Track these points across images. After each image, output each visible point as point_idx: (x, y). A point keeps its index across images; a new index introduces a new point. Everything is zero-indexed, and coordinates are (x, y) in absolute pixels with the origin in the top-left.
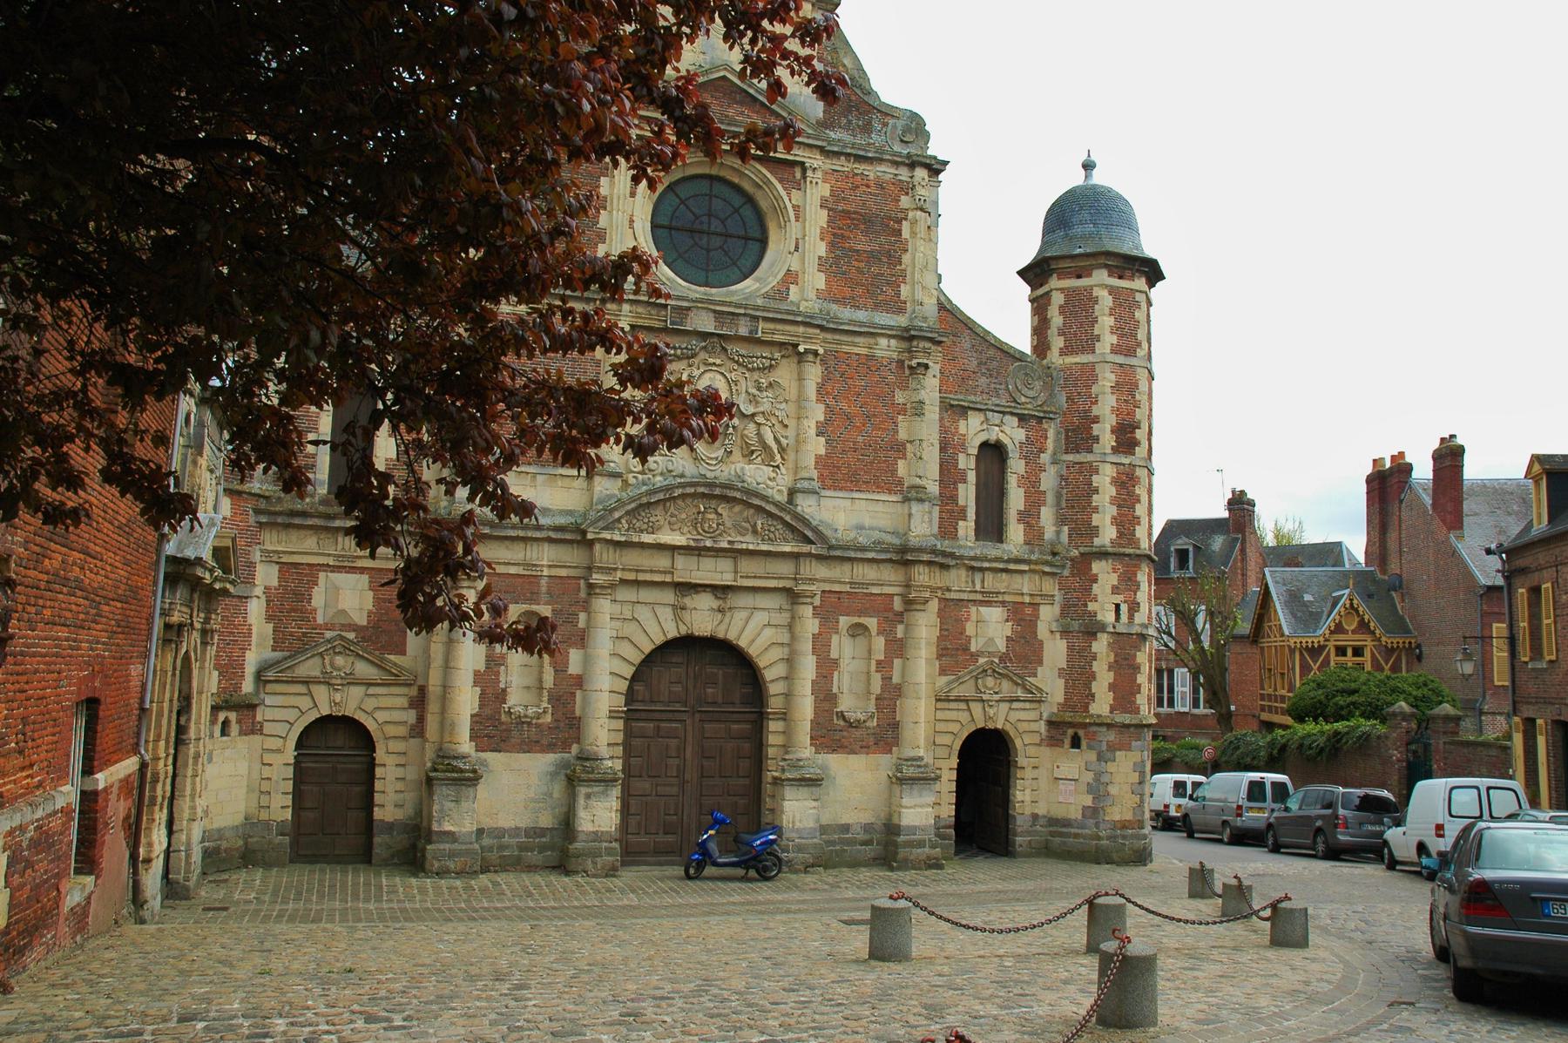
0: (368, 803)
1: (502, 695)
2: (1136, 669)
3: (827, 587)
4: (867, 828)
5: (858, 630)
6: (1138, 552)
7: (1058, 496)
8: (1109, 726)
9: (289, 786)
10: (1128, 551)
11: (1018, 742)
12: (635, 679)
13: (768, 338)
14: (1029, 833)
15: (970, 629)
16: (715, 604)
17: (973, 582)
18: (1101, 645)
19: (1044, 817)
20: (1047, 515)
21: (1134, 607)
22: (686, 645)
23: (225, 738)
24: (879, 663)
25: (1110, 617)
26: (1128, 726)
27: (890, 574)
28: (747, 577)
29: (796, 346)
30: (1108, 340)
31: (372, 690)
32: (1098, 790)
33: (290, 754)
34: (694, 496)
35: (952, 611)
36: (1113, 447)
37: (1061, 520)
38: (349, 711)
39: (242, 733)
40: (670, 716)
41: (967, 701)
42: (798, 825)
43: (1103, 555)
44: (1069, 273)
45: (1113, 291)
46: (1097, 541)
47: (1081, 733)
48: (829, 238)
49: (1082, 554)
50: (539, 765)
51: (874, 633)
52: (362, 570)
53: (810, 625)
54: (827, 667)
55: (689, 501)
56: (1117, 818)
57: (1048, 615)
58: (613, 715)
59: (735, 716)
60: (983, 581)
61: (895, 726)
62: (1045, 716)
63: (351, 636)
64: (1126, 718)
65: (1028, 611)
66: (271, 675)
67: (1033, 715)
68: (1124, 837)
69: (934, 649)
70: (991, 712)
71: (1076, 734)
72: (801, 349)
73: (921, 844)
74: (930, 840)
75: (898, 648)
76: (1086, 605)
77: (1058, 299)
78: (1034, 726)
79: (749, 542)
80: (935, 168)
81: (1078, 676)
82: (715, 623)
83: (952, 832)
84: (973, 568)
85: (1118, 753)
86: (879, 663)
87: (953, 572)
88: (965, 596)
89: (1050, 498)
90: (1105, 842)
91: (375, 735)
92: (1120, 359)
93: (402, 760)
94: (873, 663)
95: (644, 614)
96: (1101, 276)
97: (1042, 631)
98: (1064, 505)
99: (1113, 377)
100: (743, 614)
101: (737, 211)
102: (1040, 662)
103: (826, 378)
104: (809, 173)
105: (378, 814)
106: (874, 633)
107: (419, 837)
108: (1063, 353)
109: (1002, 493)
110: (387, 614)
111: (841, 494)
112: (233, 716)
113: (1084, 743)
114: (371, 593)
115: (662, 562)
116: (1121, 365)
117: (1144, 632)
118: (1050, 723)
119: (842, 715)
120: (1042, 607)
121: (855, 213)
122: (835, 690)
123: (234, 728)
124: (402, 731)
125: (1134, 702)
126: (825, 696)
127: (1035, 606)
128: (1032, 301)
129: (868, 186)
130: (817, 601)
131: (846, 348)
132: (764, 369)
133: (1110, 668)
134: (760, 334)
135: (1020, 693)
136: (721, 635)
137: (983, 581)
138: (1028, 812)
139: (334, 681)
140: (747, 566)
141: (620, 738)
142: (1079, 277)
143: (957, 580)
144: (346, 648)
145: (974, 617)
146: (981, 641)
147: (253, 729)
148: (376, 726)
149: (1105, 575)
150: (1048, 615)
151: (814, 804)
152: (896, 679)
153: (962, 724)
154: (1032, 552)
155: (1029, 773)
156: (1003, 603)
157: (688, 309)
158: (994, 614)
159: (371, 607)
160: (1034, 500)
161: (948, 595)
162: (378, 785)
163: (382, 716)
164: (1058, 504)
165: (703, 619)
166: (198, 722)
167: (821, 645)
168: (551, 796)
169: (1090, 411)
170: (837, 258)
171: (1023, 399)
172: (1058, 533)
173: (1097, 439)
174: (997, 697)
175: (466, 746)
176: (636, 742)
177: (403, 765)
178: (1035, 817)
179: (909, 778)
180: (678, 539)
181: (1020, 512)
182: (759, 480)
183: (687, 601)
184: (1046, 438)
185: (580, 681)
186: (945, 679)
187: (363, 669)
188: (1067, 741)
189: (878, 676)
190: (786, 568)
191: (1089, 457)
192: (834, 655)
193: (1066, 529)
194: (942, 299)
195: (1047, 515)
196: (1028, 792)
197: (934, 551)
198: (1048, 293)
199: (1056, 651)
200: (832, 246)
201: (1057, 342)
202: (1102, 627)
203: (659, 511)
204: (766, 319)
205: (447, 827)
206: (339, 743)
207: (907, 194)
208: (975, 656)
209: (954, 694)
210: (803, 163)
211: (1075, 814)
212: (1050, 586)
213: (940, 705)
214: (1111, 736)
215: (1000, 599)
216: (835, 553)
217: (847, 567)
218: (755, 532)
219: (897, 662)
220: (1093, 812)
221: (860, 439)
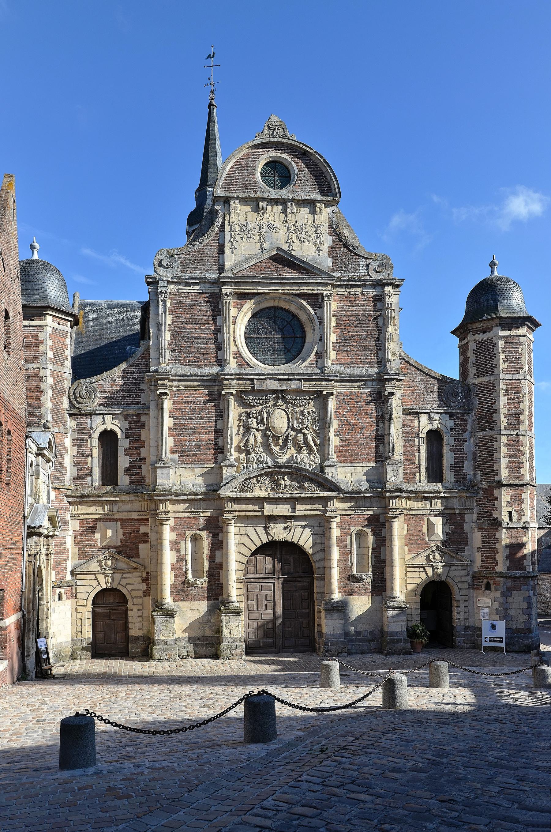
0: (126, 628)
3: (344, 512)
4: (371, 633)
6: (522, 482)
7: (475, 455)
13: (306, 389)
14: (464, 635)
20: (468, 466)
21: (521, 513)
23: (60, 601)
26: (519, 578)
28: (301, 510)
30: (503, 366)
33: (90, 607)
37: (476, 468)
40: (267, 580)
44: (479, 331)
47: (491, 582)
48: (338, 331)
52: (117, 520)
57: (471, 519)
58: (239, 581)
59: (299, 579)
64: (518, 573)
66: (79, 570)
67: (463, 573)
68: (519, 638)
69: (403, 541)
71: (488, 582)
72: (324, 393)
73: (399, 641)
74: (404, 639)
76: (492, 513)
77: (473, 346)
82: (286, 534)
85: (513, 592)
89: (470, 457)
91: (128, 597)
92: (509, 376)
93: (140, 607)
99: (505, 387)
101: (289, 323)
103: (339, 406)
104: (326, 299)
105: (132, 633)
107: (149, 643)
108: (476, 376)
109: (441, 456)
110: (129, 539)
111: (349, 465)
112: (62, 591)
113: (493, 587)
114: (122, 530)
120: (466, 515)
121: (351, 316)
123: (64, 596)
124: (140, 594)
125: (523, 564)
128: (460, 347)
132: (305, 405)
134: (302, 388)
135: (455, 562)
136: (290, 540)
138: (463, 623)
139: (107, 572)
141: (242, 592)
142: (485, 332)
148: (127, 592)
151: (341, 621)
152: (382, 558)
155: (461, 604)
157: (265, 379)
159: (122, 537)
160: (460, 457)
161: (411, 512)
162: (130, 620)
163: (130, 587)
164: (475, 459)
166: (47, 595)
168: (210, 622)
169: (491, 407)
170: (342, 341)
172: (475, 475)
173: (496, 423)
176: (250, 594)
177: (141, 610)
186: (411, 556)
188: (483, 587)
191: (492, 433)
193: (479, 472)
194: (403, 355)
195: (468, 466)
197: (401, 491)
198: (467, 343)
200: (339, 336)
201: (472, 370)
205: (162, 638)
206: (112, 601)
207: (381, 301)
210: (322, 293)
213: (408, 569)
221: (359, 436)
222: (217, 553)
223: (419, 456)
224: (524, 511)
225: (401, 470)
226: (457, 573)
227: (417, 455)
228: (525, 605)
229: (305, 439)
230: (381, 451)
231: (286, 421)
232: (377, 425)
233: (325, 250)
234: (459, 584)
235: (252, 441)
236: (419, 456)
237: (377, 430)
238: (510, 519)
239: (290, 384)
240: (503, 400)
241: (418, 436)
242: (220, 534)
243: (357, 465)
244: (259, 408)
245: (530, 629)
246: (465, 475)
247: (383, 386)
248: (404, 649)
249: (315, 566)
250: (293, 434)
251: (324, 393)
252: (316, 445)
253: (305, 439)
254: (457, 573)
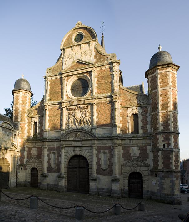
1: (50, 165)
2: (170, 159)
3: (98, 145)
4: (108, 189)
5: (105, 153)
6: (169, 132)
7: (151, 122)
8: (162, 172)
9: (30, 177)
11: (143, 175)
12: (69, 162)
15: (130, 152)
16: (80, 149)
17: (131, 142)
18: (160, 153)
19: (150, 191)
20: (148, 127)
21: (169, 144)
22: (75, 157)
24: (108, 159)
25: (162, 147)
27: (109, 142)
29: (91, 103)
31: (38, 164)
32: (161, 186)
34: (75, 132)
35: (126, 148)
36: (161, 109)
37: (152, 127)
38: (35, 167)
39: (24, 169)
41: (130, 166)
42: (92, 187)
43: (160, 133)
46: (158, 131)
47: (157, 173)
49: (156, 134)
50: (55, 175)
51: (107, 153)
53: (95, 152)
54: (99, 159)
55: (74, 133)
56: (166, 193)
58: (65, 168)
60: (133, 142)
61: (112, 171)
62: (149, 170)
63: (35, 157)
65: (144, 147)
66: (27, 162)
67: (146, 169)
70: (136, 168)
72: (92, 104)
73: (116, 193)
75: (112, 156)
76: (157, 145)
78: (146, 172)
79: (83, 138)
81: (156, 160)
83: (128, 192)
84: (130, 139)
85: (165, 178)
86: (108, 159)
87: (126, 141)
88: (129, 145)
89: (149, 123)
90: (162, 198)
94: (107, 159)
95: (69, 152)
97: (148, 151)
98: (152, 124)
100: (84, 151)
102: (148, 158)
106: (107, 153)
112: (23, 167)
115: (70, 143)
116: (163, 90)
117: (172, 150)
118: (151, 171)
119: (101, 168)
120: (148, 146)
122: (100, 164)
123: (23, 169)
126: (98, 164)
127: (146, 146)
129: (104, 71)
130: (96, 148)
131: (101, 102)
133: (162, 159)
135: (143, 165)
136: (81, 155)
137: (133, 142)
138: (146, 190)
140: (84, 142)
143: (127, 142)
144: (34, 158)
145: (131, 149)
146: (133, 154)
147: (25, 169)
149: (160, 138)
150: (149, 148)
152: (112, 162)
153: (128, 171)
154: (145, 135)
155: (146, 181)
156: (138, 146)
158: (135, 149)
161: (125, 145)
164: (151, 124)
165: (78, 152)
167: (97, 156)
171: (142, 103)
172: (151, 130)
174: (137, 165)
175: (46, 171)
178: (148, 191)
179: (116, 180)
180: (72, 139)
181: (141, 127)
182: (86, 127)
183: (75, 149)
184: (148, 110)
185: (60, 162)
186: (125, 162)
187: (37, 161)
188: (154, 175)
189: (109, 161)
190: (90, 142)
191: (156, 112)
192: (100, 157)
193: (152, 129)
195: (148, 127)
196: (146, 185)
199: (151, 156)
202: (160, 150)
203: (70, 135)
204: (86, 100)
208: (132, 157)
209: (128, 164)
211: (156, 191)
212: (149, 142)
214: (163, 174)
215: (137, 145)
216: (98, 139)
217: (102, 141)
218: (85, 137)
219: (112, 158)
222: (59, 158)
223: (128, 124)
224: (170, 144)
226: (144, 169)
227: (127, 124)
228: (171, 184)
229: (86, 120)
230: (112, 122)
231: (80, 115)
232: (111, 113)
233: (93, 57)
234: (144, 174)
235: (70, 122)
236: (128, 124)
237: (111, 115)
238: (164, 147)
239: (81, 102)
240: (160, 98)
241: (128, 116)
242: (60, 152)
243: (103, 128)
244: (72, 111)
245: (174, 194)
246: (147, 130)
247: (112, 99)
248: (118, 196)
249: (89, 163)
250: (82, 118)
251: (92, 104)
252: (90, 122)
253: (86, 120)
254: (144, 169)
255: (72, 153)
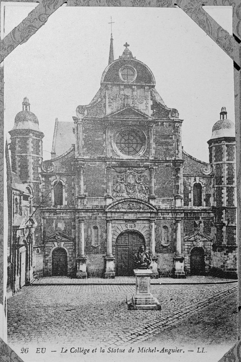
10: (232, 207)
18: (224, 229)
31: (65, 242)
45: (227, 145)
72: (149, 168)
77: (214, 148)
80: (181, 122)
96: (223, 142)
112: (39, 249)
128: (209, 148)
165: (130, 227)
181: (204, 199)
191: (221, 186)
195: (211, 199)
201: (214, 159)
220: (223, 266)
225: (183, 200)
255: (123, 227)
